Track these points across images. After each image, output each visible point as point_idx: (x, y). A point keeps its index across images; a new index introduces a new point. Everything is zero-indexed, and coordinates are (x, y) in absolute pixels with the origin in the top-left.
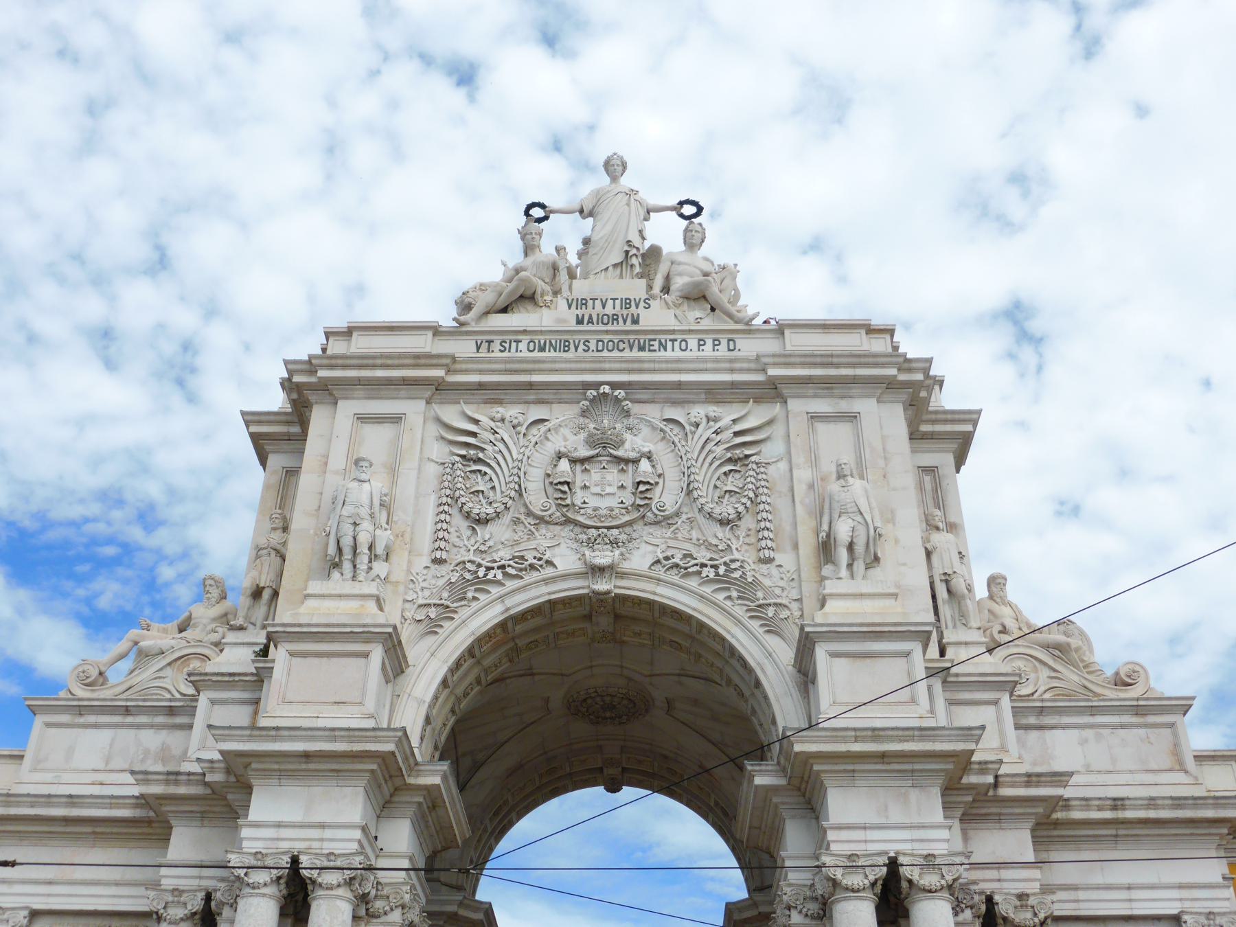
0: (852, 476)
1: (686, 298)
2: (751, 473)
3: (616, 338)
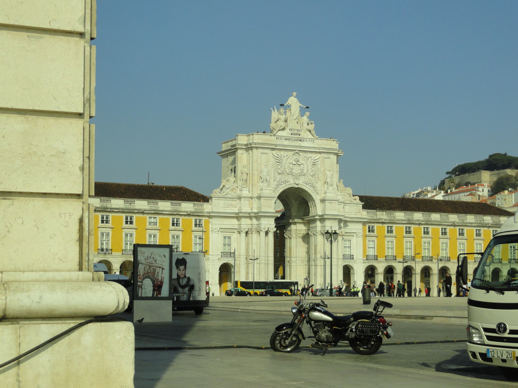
0: (330, 171)
1: (307, 130)
2: (316, 167)
3: (297, 138)
